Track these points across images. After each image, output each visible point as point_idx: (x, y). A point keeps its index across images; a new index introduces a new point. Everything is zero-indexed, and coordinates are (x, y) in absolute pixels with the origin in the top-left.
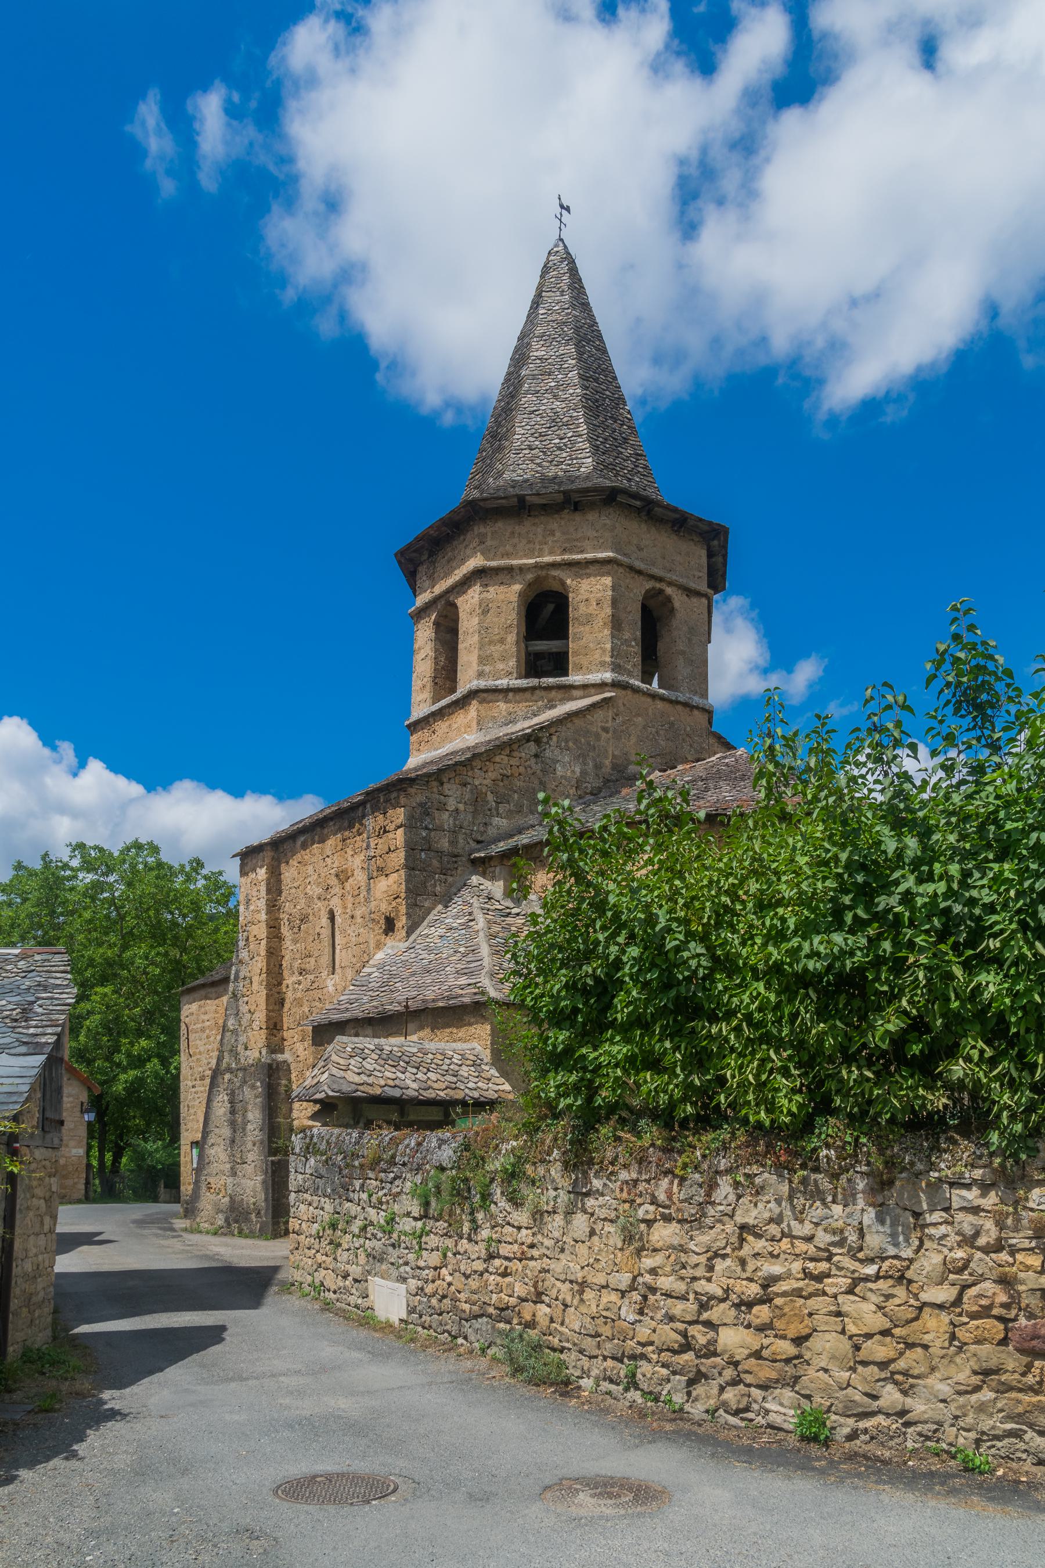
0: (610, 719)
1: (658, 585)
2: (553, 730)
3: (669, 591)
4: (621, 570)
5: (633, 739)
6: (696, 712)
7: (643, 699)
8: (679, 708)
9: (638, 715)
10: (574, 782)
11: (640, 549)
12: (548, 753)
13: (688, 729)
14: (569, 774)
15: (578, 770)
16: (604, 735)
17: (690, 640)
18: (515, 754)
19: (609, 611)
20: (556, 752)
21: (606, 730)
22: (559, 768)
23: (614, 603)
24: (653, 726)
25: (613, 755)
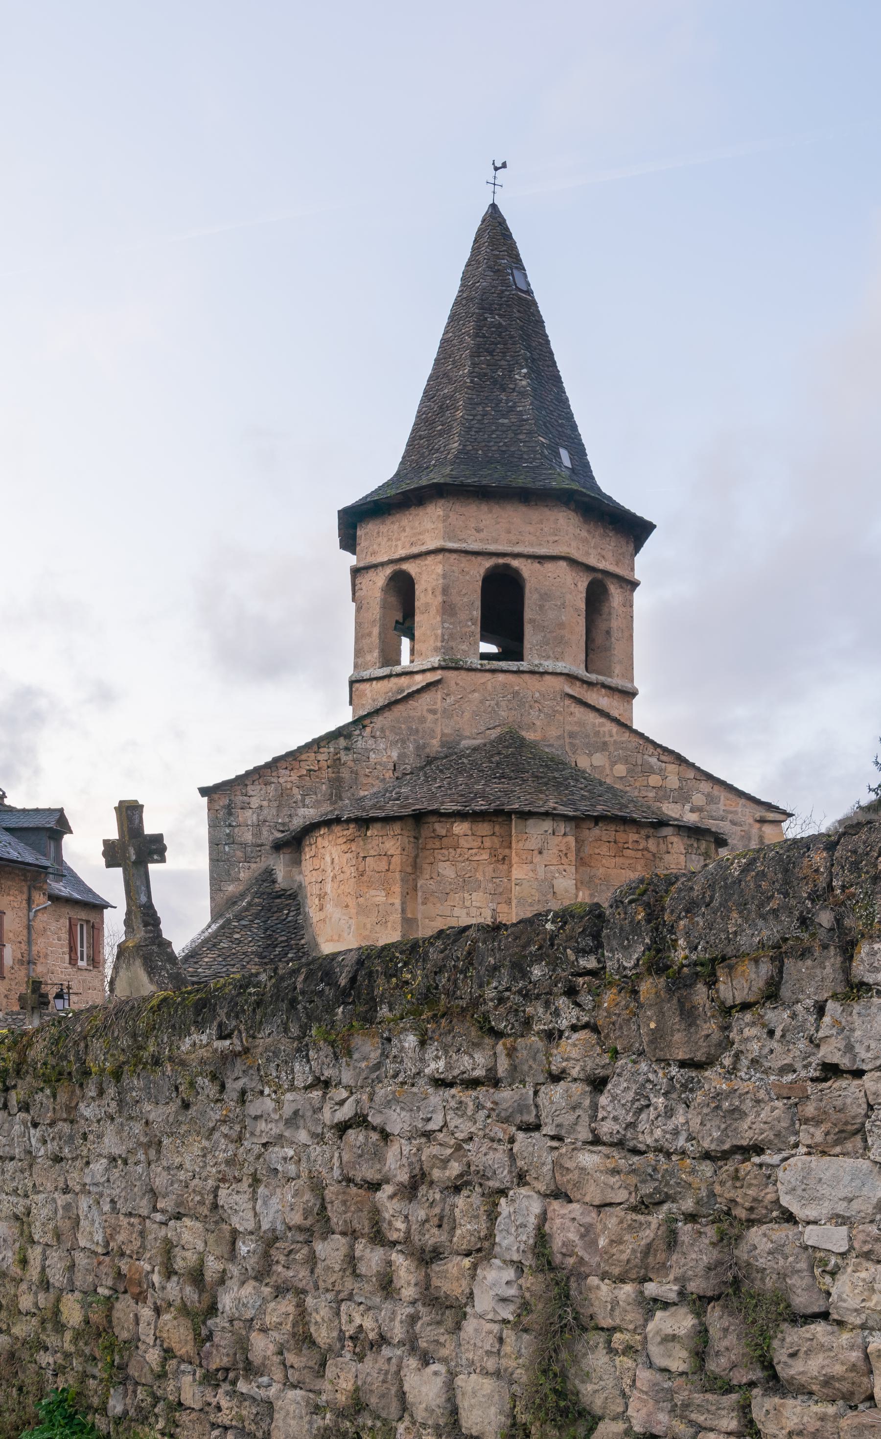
0: (439, 701)
1: (501, 561)
2: (367, 722)
3: (515, 563)
4: (454, 556)
5: (467, 715)
6: (547, 678)
7: (479, 675)
8: (526, 677)
9: (474, 691)
10: (391, 766)
11: (478, 530)
12: (360, 744)
13: (537, 695)
14: (384, 759)
15: (395, 755)
16: (430, 717)
17: (541, 607)
18: (321, 750)
19: (440, 599)
20: (370, 742)
21: (433, 712)
22: (372, 755)
23: (445, 591)
24: (492, 699)
25: (443, 735)
